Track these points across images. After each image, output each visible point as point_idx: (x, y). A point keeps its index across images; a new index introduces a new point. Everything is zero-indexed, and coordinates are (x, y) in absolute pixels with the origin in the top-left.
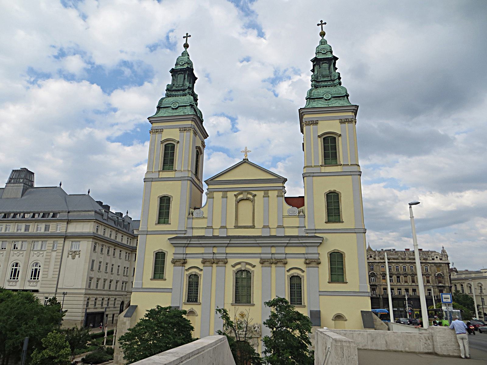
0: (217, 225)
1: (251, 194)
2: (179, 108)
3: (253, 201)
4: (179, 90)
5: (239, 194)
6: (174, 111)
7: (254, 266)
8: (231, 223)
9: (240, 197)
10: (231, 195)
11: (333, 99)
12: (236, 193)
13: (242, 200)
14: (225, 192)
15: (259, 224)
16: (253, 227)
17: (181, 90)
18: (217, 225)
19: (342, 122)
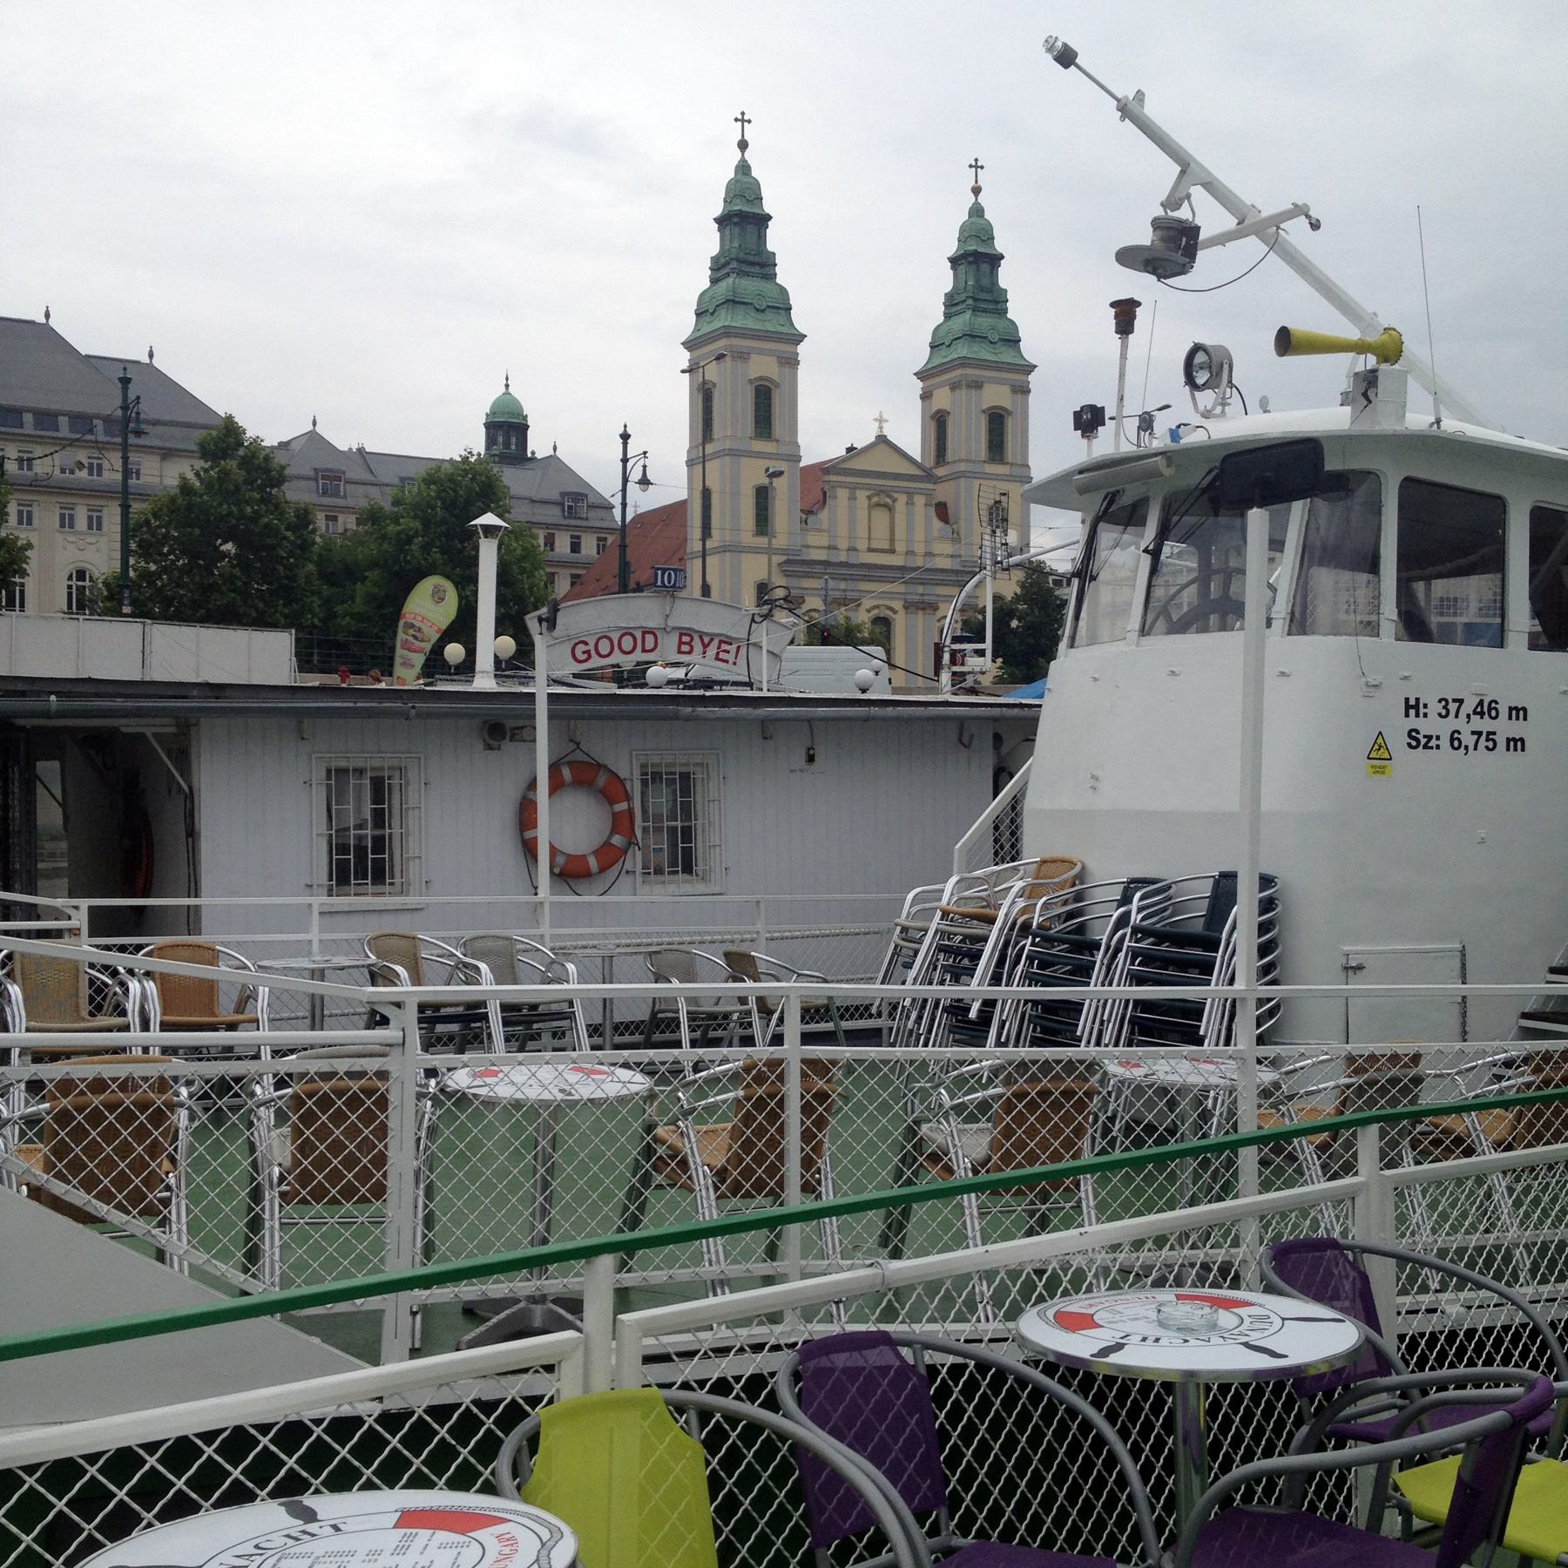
0: (843, 544)
1: (889, 496)
3: (890, 509)
4: (753, 264)
6: (760, 316)
7: (895, 612)
8: (862, 545)
9: (875, 499)
10: (862, 495)
11: (1000, 343)
12: (869, 493)
13: (878, 505)
14: (853, 488)
16: (892, 551)
17: (758, 264)
18: (843, 544)
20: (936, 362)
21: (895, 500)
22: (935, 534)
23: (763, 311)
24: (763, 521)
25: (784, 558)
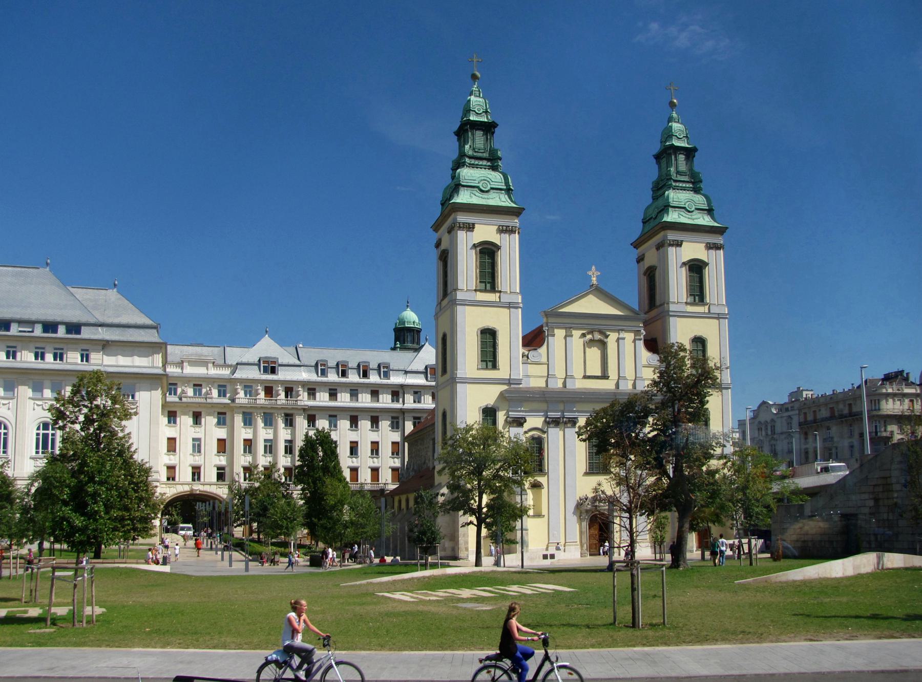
2: (492, 191)
5: (588, 333)
6: (485, 196)
8: (577, 372)
9: (589, 337)
11: (697, 211)
16: (605, 376)
19: (710, 247)
20: (646, 230)
21: (607, 337)
23: (487, 192)
24: (489, 356)
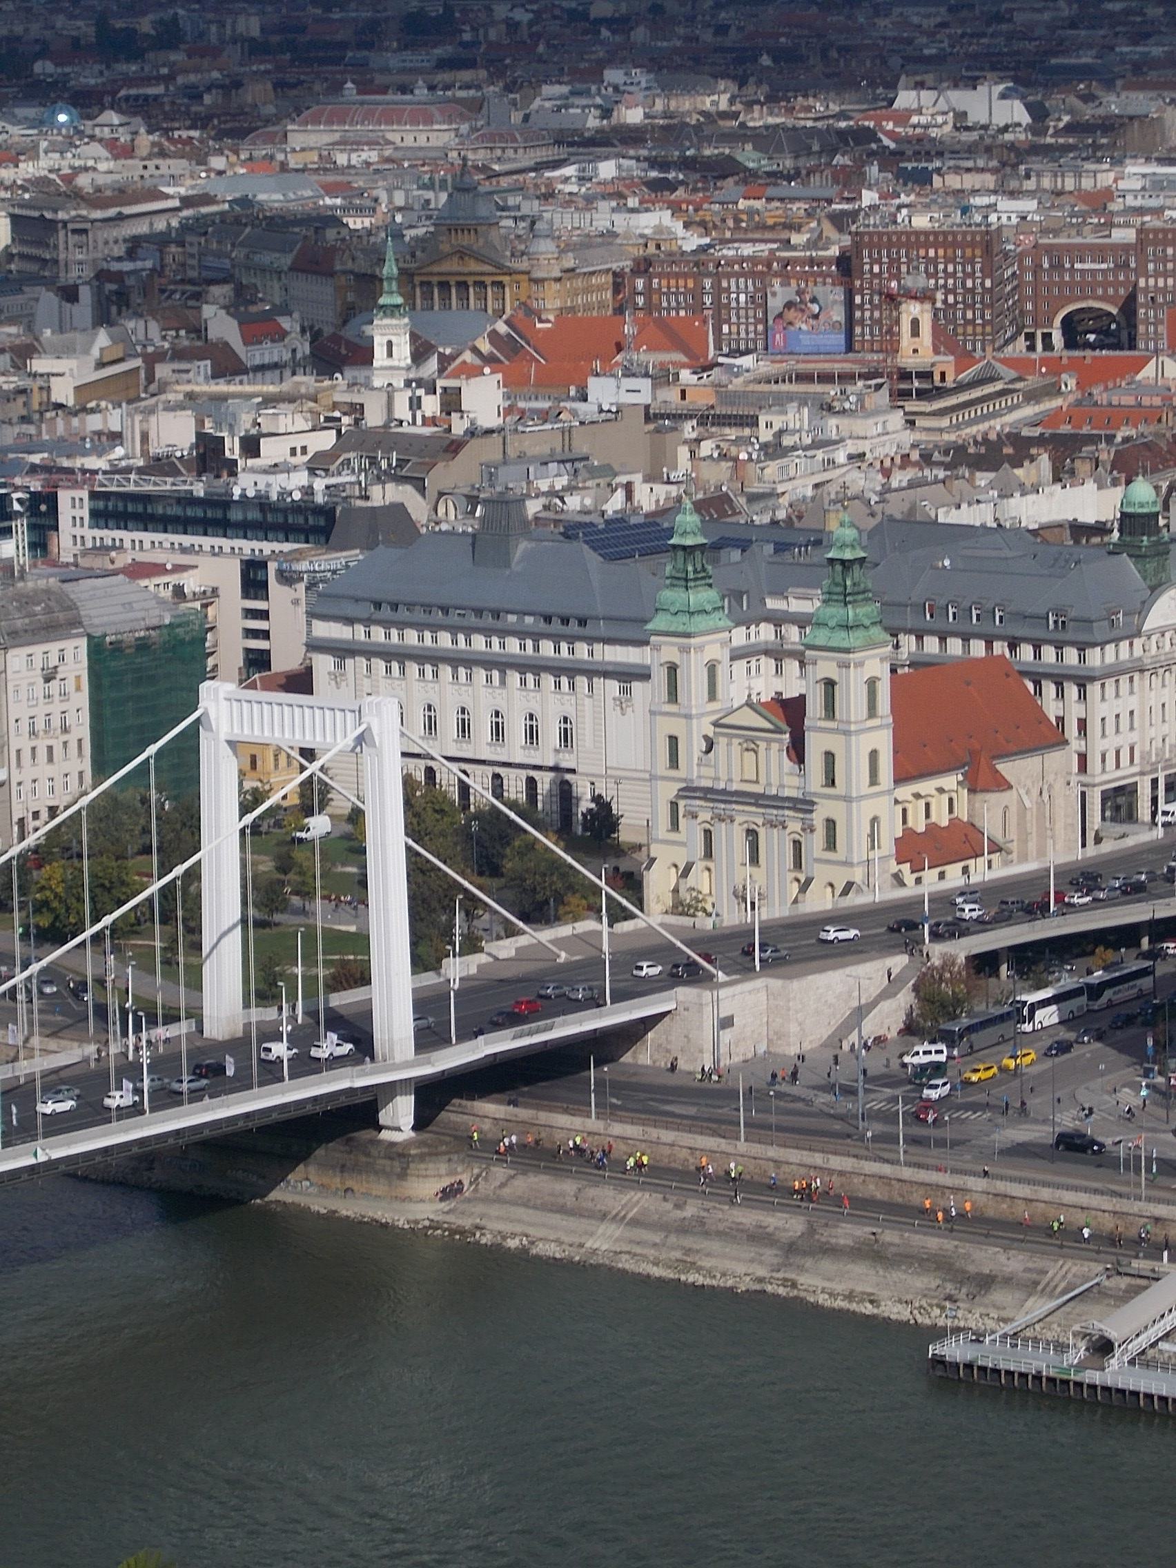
3: (756, 752)
8: (736, 776)
9: (745, 745)
15: (763, 780)
16: (757, 782)
18: (723, 776)
22: (786, 770)
25: (684, 785)
